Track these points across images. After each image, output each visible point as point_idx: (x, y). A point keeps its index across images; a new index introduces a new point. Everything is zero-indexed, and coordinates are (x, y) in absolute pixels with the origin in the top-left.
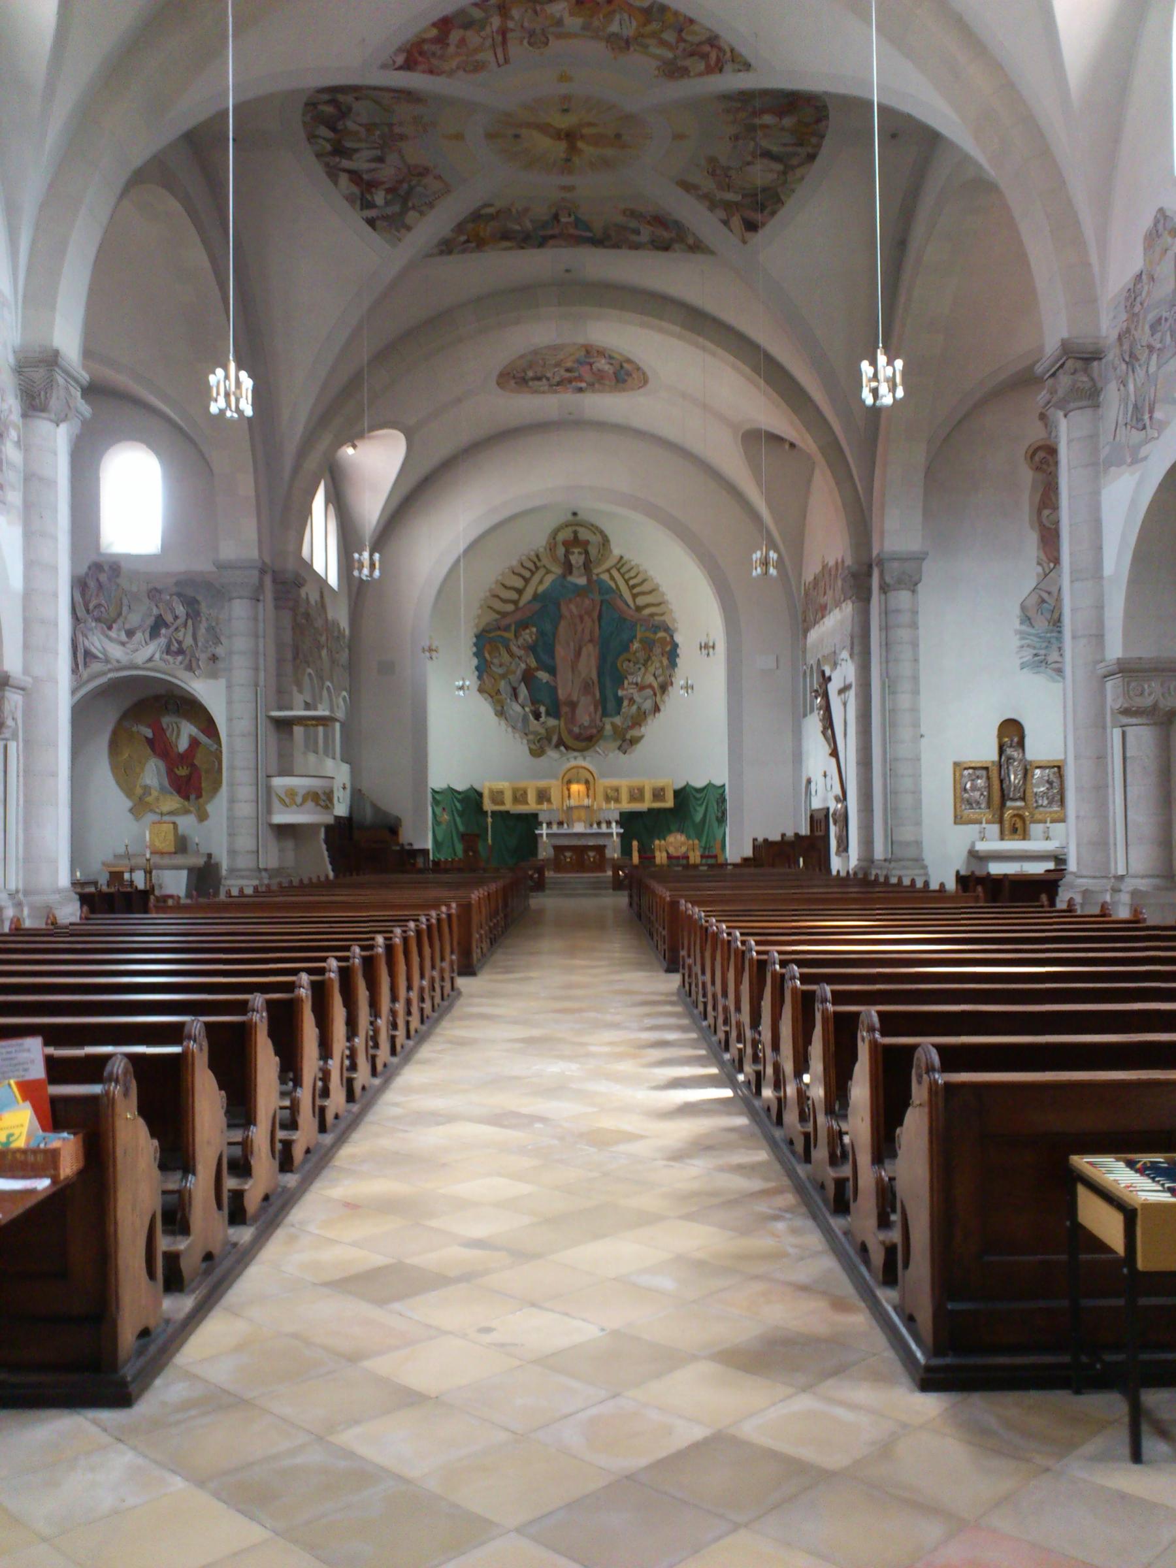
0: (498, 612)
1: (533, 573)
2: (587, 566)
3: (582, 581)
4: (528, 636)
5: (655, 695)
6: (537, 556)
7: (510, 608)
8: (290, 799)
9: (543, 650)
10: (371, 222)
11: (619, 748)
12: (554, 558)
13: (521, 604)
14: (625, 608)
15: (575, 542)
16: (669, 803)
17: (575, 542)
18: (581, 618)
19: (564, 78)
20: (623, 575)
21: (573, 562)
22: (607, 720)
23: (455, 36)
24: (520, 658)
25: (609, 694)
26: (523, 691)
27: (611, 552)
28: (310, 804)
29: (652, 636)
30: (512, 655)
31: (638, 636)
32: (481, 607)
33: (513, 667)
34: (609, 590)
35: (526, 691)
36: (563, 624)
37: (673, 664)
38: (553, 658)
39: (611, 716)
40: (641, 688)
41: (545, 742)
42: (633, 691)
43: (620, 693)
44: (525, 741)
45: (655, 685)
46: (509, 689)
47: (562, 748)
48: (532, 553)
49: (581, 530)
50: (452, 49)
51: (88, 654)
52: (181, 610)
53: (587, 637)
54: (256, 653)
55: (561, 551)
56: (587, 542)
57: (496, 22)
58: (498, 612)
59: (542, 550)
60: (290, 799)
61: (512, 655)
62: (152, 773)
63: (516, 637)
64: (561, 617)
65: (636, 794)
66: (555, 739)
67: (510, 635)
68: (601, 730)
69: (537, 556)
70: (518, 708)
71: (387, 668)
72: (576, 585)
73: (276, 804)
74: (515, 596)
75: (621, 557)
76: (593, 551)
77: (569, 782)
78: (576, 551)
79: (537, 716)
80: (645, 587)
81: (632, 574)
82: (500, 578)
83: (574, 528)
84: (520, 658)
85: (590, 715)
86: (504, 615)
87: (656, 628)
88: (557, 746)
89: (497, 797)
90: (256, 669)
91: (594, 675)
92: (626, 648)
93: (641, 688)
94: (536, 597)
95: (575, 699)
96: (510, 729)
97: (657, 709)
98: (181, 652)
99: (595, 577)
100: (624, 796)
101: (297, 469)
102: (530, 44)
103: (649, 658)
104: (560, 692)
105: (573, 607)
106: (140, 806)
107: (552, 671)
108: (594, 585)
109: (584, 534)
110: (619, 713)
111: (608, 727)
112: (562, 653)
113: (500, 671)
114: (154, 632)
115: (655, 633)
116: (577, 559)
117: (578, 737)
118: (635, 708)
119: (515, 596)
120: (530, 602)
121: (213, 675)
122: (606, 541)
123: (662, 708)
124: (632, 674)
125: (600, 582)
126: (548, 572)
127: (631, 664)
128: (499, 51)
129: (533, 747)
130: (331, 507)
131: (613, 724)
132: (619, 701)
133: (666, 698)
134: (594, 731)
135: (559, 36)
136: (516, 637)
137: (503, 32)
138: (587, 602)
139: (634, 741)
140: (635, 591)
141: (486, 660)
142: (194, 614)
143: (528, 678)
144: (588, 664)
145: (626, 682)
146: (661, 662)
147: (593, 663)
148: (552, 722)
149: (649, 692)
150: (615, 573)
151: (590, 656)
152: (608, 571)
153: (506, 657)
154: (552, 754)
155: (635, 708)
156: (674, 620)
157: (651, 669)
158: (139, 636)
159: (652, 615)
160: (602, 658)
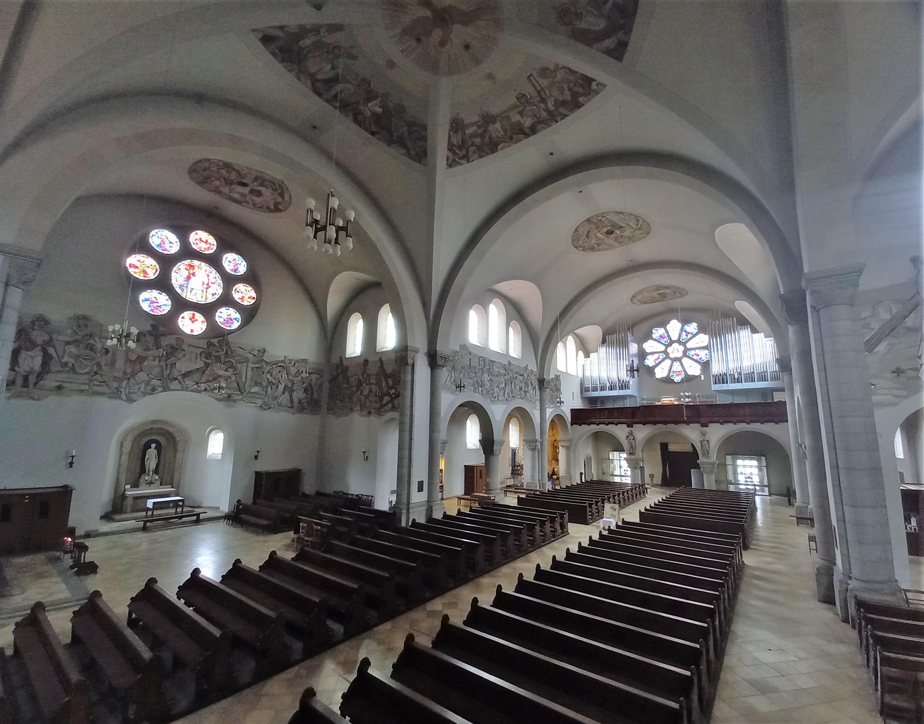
19: (490, 77)
23: (567, 96)
50: (565, 86)
57: (552, 108)
102: (524, 95)
128: (539, 88)
135: (515, 107)
137: (543, 101)
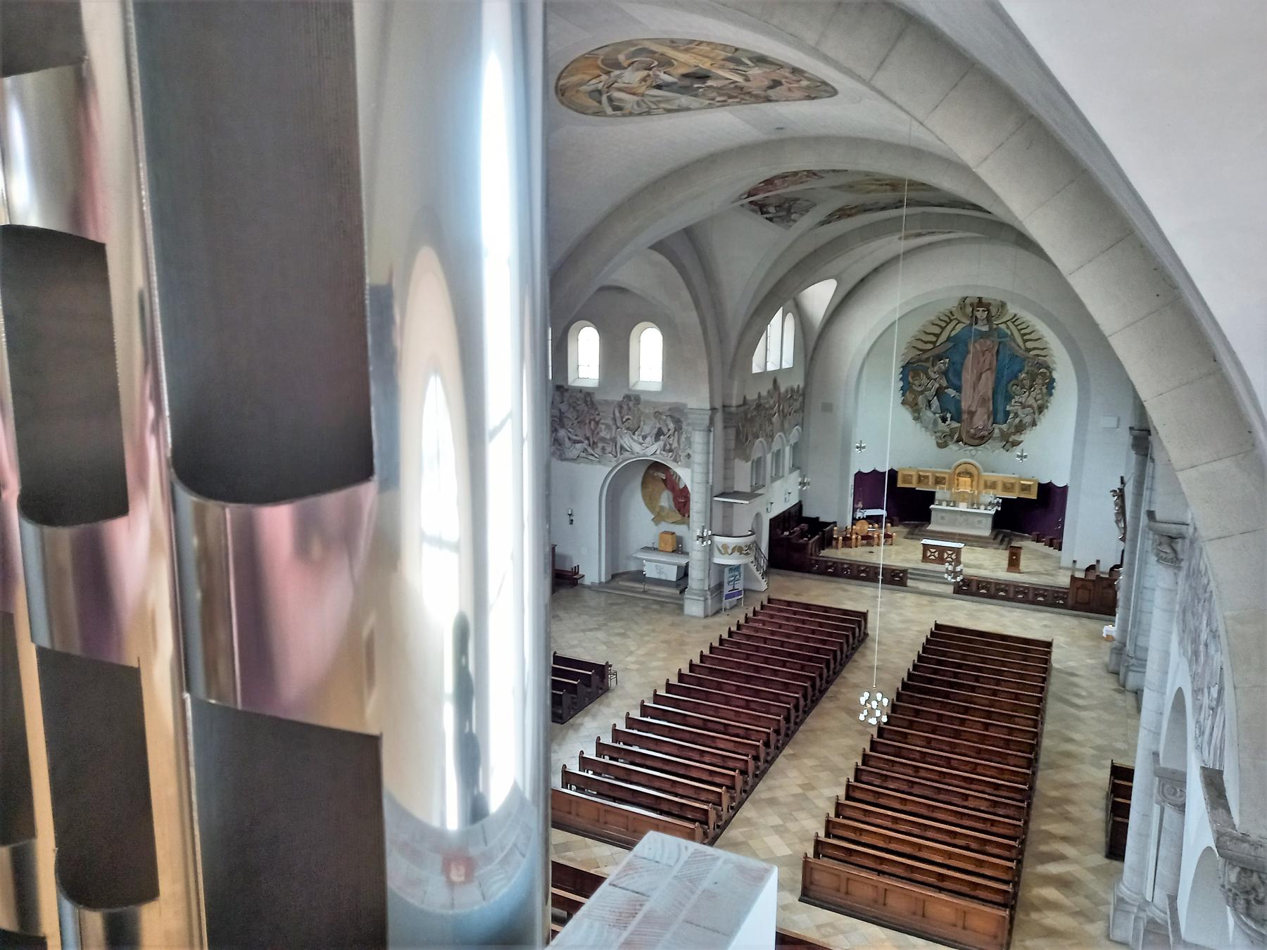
1: (948, 324)
2: (989, 319)
3: (985, 329)
4: (942, 365)
7: (931, 346)
8: (724, 550)
9: (953, 376)
10: (770, 219)
12: (965, 315)
16: (1034, 496)
25: (1000, 408)
28: (736, 554)
30: (929, 378)
34: (1006, 335)
37: (1051, 394)
40: (1024, 406)
43: (1008, 408)
45: (1035, 405)
51: (622, 447)
52: (672, 426)
54: (708, 463)
60: (724, 550)
61: (929, 378)
62: (666, 499)
64: (968, 352)
65: (1006, 488)
67: (929, 364)
68: (991, 433)
71: (828, 408)
73: (716, 552)
74: (934, 339)
76: (994, 311)
77: (959, 475)
79: (944, 420)
80: (1032, 336)
86: (925, 351)
87: (1040, 365)
88: (958, 441)
89: (907, 478)
90: (708, 473)
91: (990, 394)
92: (1016, 377)
93: (1024, 406)
94: (949, 339)
97: (1034, 424)
98: (670, 451)
100: (1000, 486)
101: (740, 342)
105: (977, 346)
106: (658, 519)
111: (997, 431)
112: (968, 377)
113: (920, 389)
114: (657, 438)
116: (981, 314)
117: (973, 437)
118: (1017, 420)
119: (934, 339)
121: (688, 466)
130: (790, 317)
132: (1007, 414)
138: (988, 342)
139: (1016, 444)
142: (678, 429)
143: (939, 393)
144: (987, 382)
147: (990, 385)
149: (1029, 410)
153: (925, 380)
154: (953, 447)
155: (1017, 420)
158: (648, 439)
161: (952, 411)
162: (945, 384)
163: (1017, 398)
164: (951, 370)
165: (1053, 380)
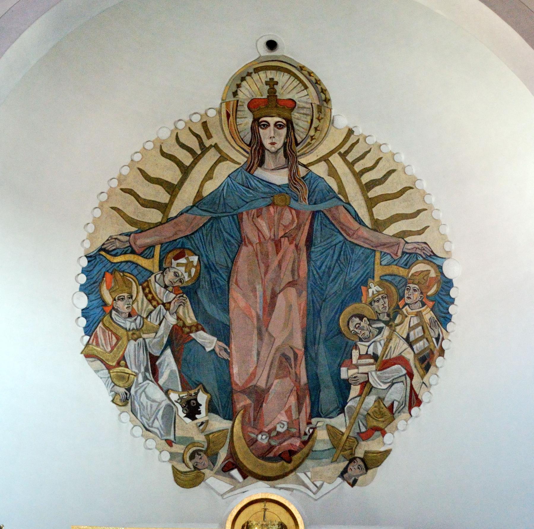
0: (132, 222)
1: (197, 158)
2: (290, 151)
3: (280, 178)
4: (185, 269)
5: (411, 375)
6: (205, 125)
7: (154, 216)
9: (209, 291)
11: (343, 474)
12: (235, 134)
13: (173, 212)
14: (356, 225)
15: (270, 104)
17: (270, 104)
18: (278, 244)
20: (351, 165)
21: (266, 143)
22: (320, 422)
24: (166, 305)
25: (326, 379)
26: (168, 363)
27: (332, 122)
29: (402, 272)
30: (152, 299)
31: (379, 271)
32: (101, 206)
33: (153, 320)
34: (329, 194)
35: (174, 367)
36: (245, 251)
37: (444, 318)
38: (226, 310)
39: (328, 415)
40: (383, 364)
41: (205, 459)
42: (368, 368)
43: (345, 373)
44: (166, 456)
45: (409, 356)
46: (143, 357)
47: (235, 473)
48: (196, 118)
49: (281, 78)
53: (287, 278)
55: (246, 120)
56: (292, 104)
58: (132, 222)
59: (212, 113)
63: (163, 270)
64: (242, 241)
66: (223, 454)
69: (205, 125)
70: (159, 395)
72: (269, 184)
74: (163, 197)
75: (350, 132)
76: (301, 123)
78: (272, 120)
79: (192, 411)
80: (391, 186)
81: (367, 162)
82: (138, 157)
83: (271, 74)
84: (166, 305)
85: (288, 412)
86: (143, 228)
88: (226, 469)
91: (298, 343)
92: (355, 294)
93: (383, 364)
94: (199, 201)
95: (262, 383)
96: (139, 431)
97: (414, 400)
99: (302, 171)
103: (397, 310)
104: (235, 370)
105: (263, 224)
107: (223, 333)
108: (301, 184)
109: (288, 88)
110: (342, 411)
111: (322, 435)
113: (129, 324)
115: (407, 266)
116: (273, 138)
118: (371, 400)
119: (163, 197)
120: (187, 210)
122: (325, 100)
123: (424, 396)
124: (367, 339)
125: (312, 180)
126: (223, 158)
127: (364, 323)
129: (182, 468)
131: (332, 431)
132: (343, 387)
133: (431, 378)
134: (297, 442)
136: (163, 270)
138: (288, 216)
139: (371, 462)
140: (372, 194)
141: (105, 304)
143: (178, 339)
145: (355, 354)
146: (419, 315)
148: (218, 424)
149: (398, 370)
150: (336, 160)
151: (291, 306)
152: (325, 159)
153: (141, 303)
154: (215, 483)
155: (371, 400)
156: (444, 238)
157: (402, 330)
159: (403, 234)
160: (313, 313)
161: (211, 388)
162: (190, 318)
163: (363, 347)
164: (205, 284)
165: (448, 284)
